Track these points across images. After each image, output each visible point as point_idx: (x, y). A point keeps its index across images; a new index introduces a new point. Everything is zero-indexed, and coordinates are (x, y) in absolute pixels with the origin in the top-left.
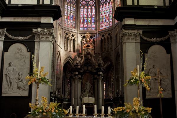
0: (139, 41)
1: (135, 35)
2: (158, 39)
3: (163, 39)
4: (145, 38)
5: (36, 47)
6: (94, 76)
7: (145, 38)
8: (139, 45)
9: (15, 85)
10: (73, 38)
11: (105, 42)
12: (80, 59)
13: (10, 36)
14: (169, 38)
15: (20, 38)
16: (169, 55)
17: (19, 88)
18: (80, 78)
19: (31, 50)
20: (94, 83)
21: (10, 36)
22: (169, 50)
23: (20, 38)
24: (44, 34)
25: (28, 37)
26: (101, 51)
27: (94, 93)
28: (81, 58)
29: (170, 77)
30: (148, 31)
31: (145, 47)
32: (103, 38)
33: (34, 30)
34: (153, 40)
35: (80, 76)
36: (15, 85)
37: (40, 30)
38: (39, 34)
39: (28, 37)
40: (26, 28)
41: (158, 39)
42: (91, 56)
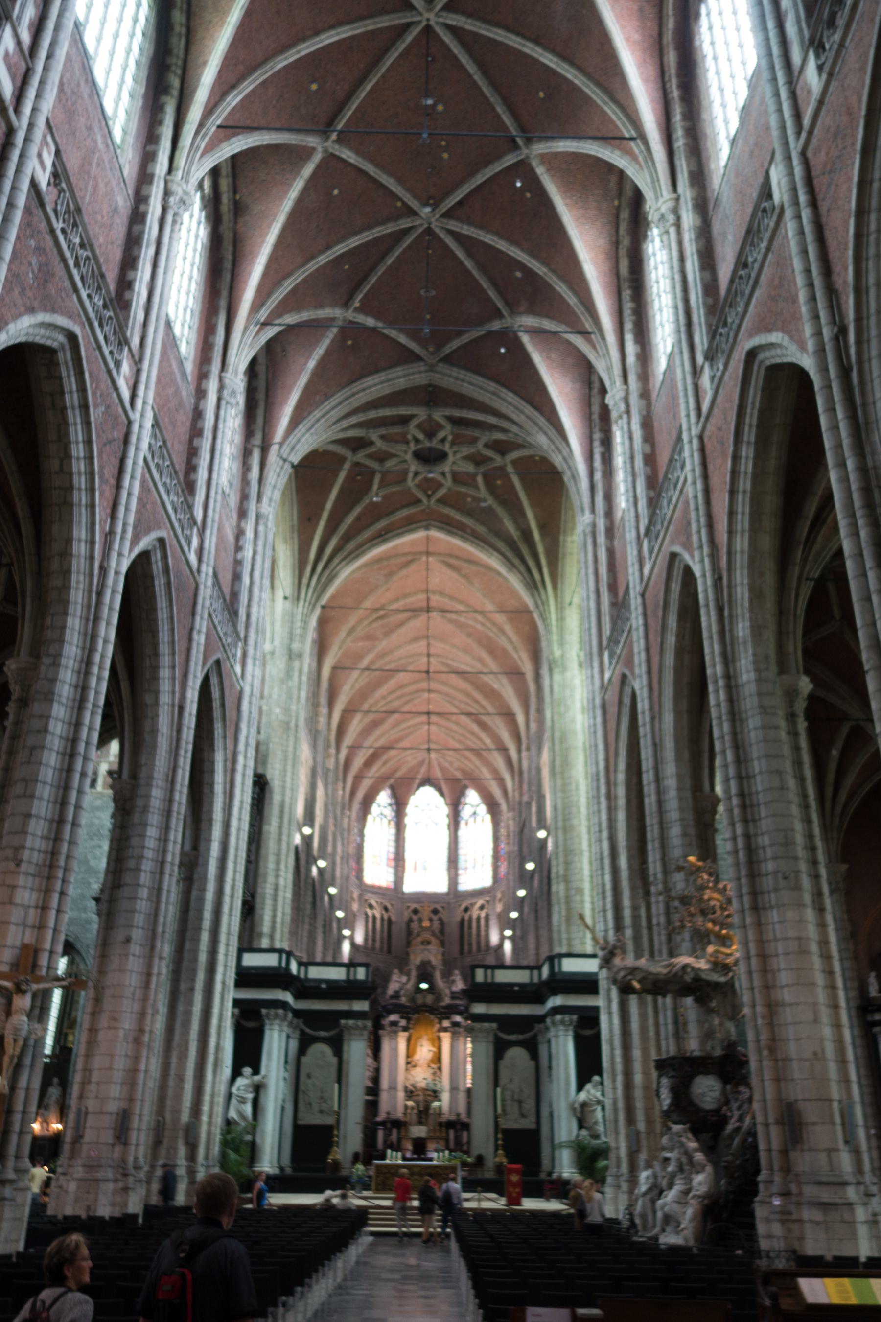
0: (491, 1039)
1: (487, 1031)
2: (520, 1037)
3: (528, 1035)
4: (502, 1035)
5: (345, 1048)
6: (440, 1023)
7: (502, 1035)
8: (491, 1047)
9: (316, 1107)
10: (386, 917)
11: (470, 927)
12: (404, 979)
13: (308, 1030)
14: (535, 1036)
15: (323, 1034)
16: (532, 1064)
17: (321, 1112)
18: (405, 1029)
19: (338, 1051)
20: (439, 1039)
21: (308, 1030)
22: (534, 1055)
23: (323, 1034)
24: (357, 1028)
25: (332, 1033)
26: (462, 952)
27: (440, 1069)
28: (408, 974)
29: (533, 1097)
30: (506, 1023)
31: (500, 1049)
32: (467, 917)
33: (343, 1022)
34: (513, 1037)
35: (403, 1023)
36: (316, 1107)
37: (351, 1022)
38: (349, 1028)
39: (332, 1033)
40: (331, 1019)
41: (520, 1037)
42: (433, 968)
